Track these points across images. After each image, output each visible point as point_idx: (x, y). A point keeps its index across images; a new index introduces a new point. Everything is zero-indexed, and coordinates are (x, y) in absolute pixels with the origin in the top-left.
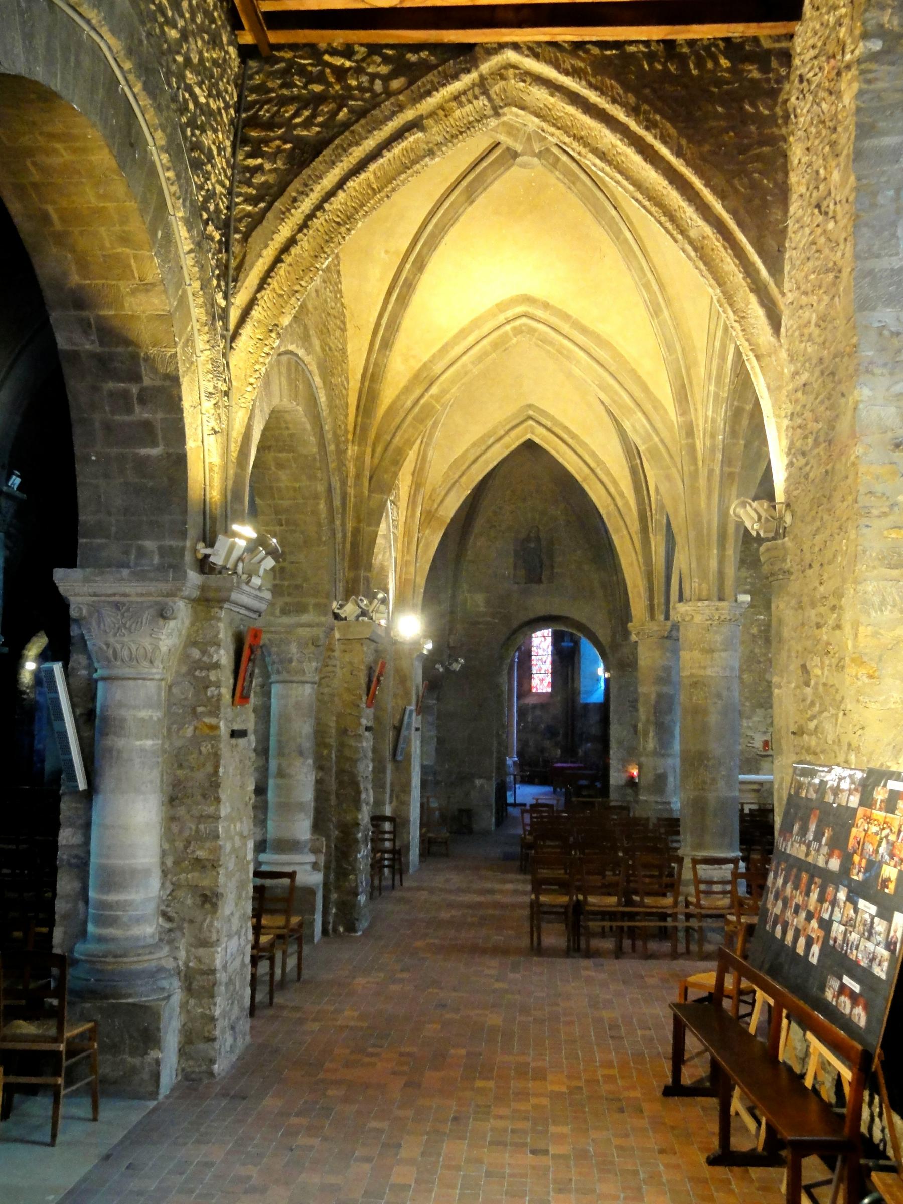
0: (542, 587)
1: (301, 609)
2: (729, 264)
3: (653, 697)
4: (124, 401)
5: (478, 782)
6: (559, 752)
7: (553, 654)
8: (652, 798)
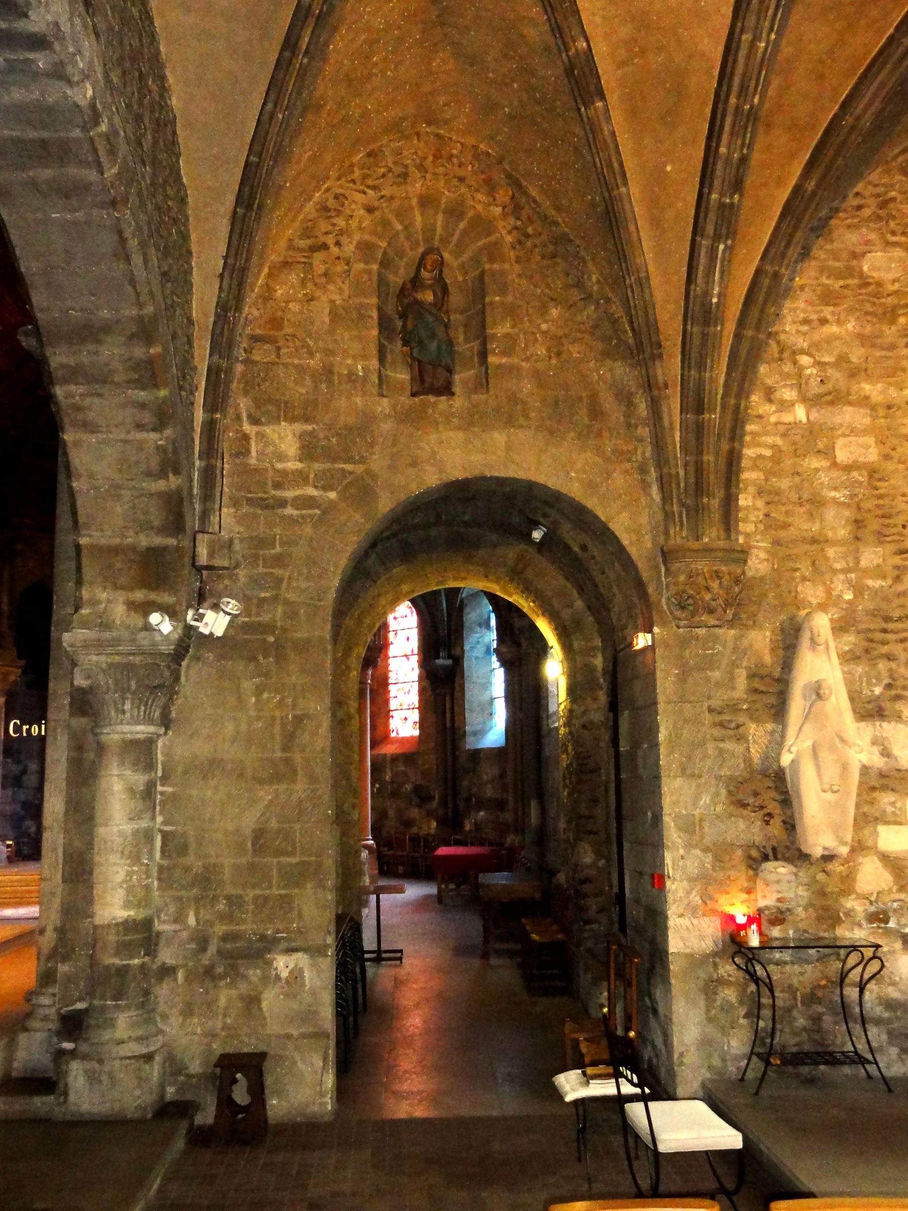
0: (459, 402)
5: (283, 964)
6: (434, 824)
7: (420, 680)
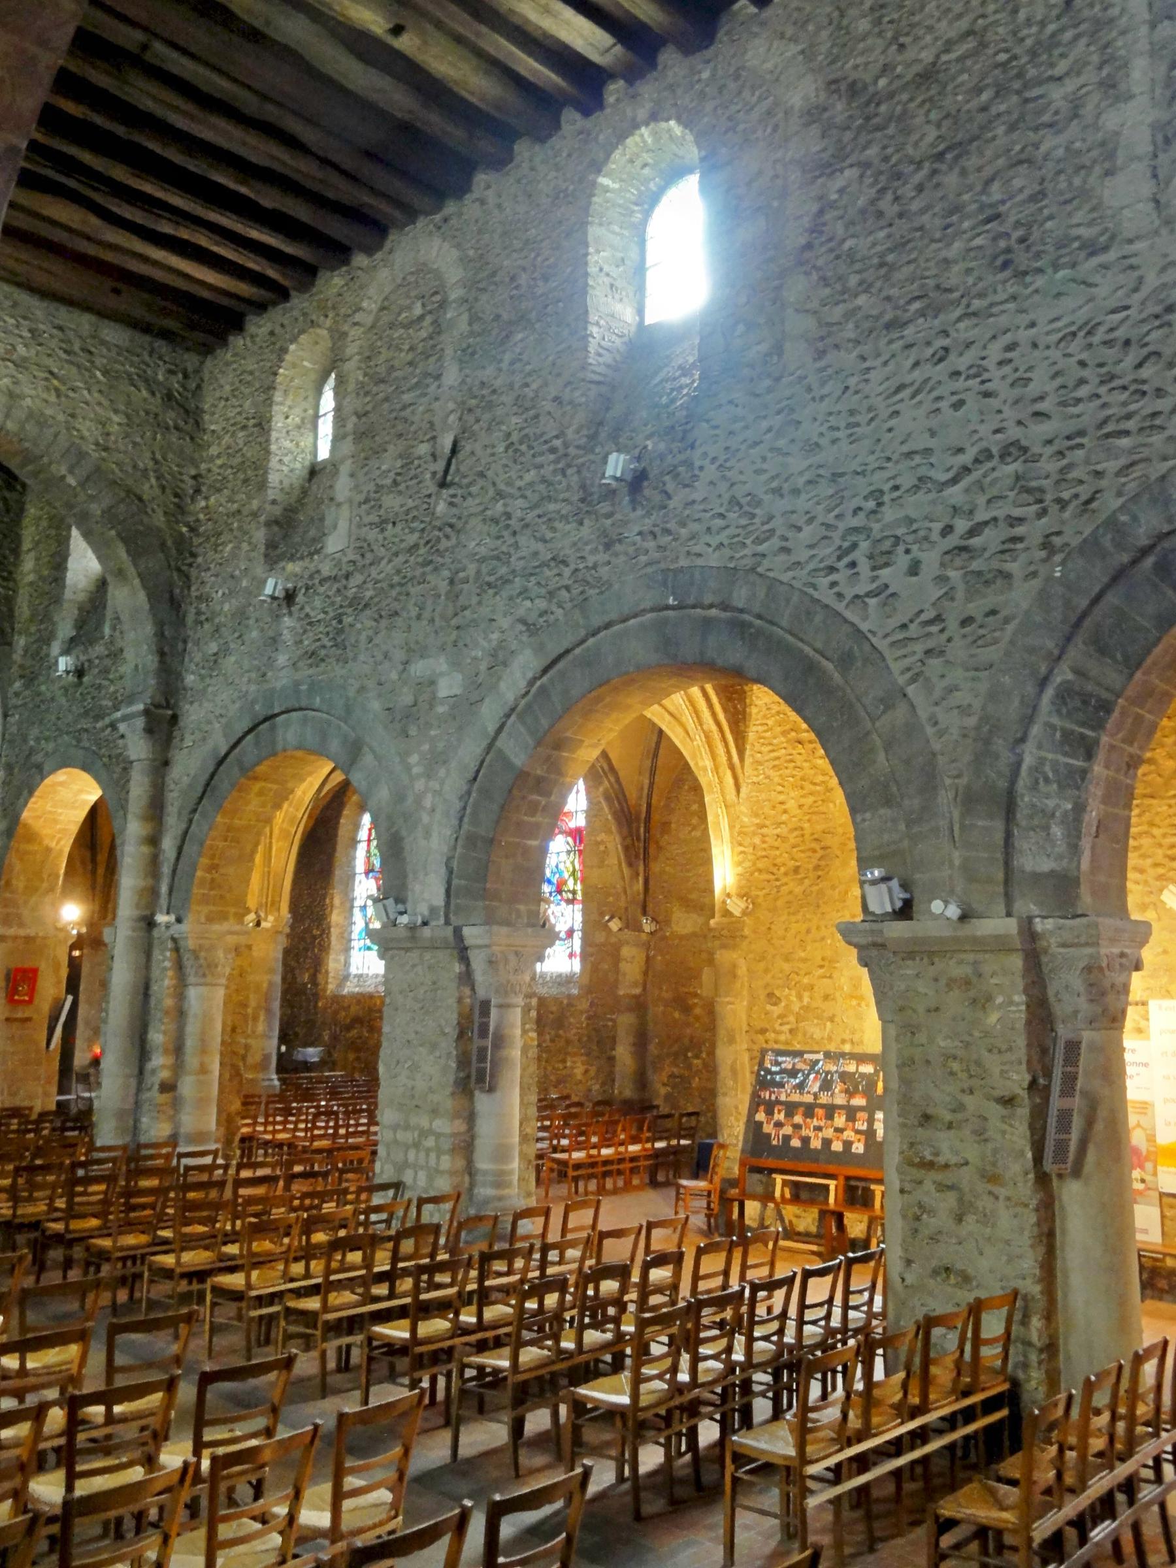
1: (224, 917)
2: (720, 750)
3: (265, 985)
4: (534, 809)
8: (261, 1076)
